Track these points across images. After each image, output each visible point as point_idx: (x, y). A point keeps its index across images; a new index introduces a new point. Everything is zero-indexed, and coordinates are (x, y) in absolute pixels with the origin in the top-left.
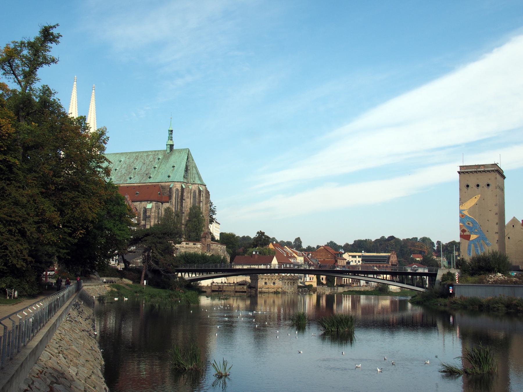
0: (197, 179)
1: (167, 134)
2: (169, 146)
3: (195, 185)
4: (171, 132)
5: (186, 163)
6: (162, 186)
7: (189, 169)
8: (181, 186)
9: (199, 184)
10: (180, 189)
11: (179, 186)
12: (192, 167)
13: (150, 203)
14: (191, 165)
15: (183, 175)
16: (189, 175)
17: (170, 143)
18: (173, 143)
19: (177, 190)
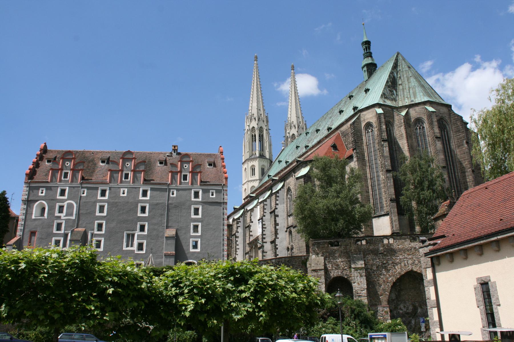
0: (421, 94)
1: (361, 51)
2: (365, 69)
3: (417, 108)
4: (365, 44)
5: (392, 73)
6: (343, 133)
7: (400, 83)
8: (374, 114)
9: (425, 103)
10: (374, 121)
11: (371, 116)
12: (406, 79)
13: (306, 166)
14: (405, 76)
15: (381, 94)
16: (400, 93)
17: (369, 61)
18: (373, 60)
19: (369, 125)
